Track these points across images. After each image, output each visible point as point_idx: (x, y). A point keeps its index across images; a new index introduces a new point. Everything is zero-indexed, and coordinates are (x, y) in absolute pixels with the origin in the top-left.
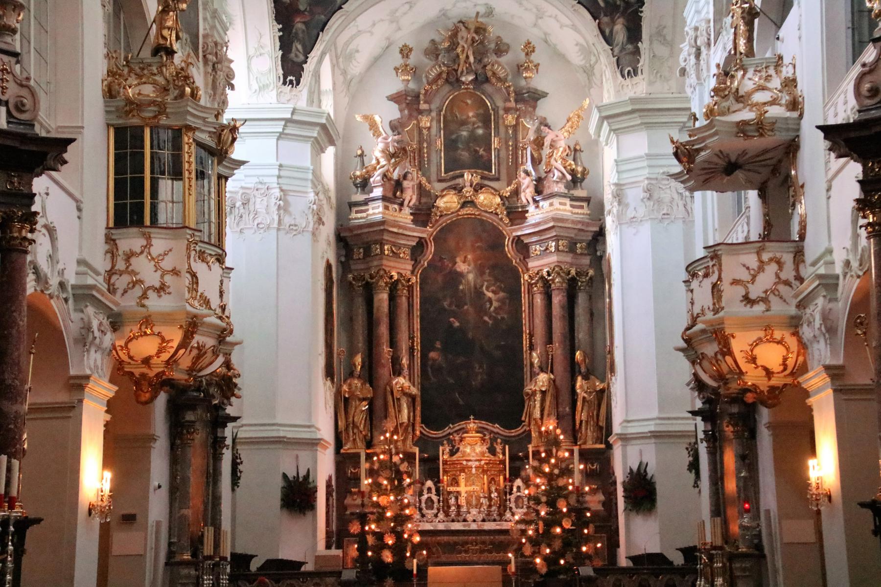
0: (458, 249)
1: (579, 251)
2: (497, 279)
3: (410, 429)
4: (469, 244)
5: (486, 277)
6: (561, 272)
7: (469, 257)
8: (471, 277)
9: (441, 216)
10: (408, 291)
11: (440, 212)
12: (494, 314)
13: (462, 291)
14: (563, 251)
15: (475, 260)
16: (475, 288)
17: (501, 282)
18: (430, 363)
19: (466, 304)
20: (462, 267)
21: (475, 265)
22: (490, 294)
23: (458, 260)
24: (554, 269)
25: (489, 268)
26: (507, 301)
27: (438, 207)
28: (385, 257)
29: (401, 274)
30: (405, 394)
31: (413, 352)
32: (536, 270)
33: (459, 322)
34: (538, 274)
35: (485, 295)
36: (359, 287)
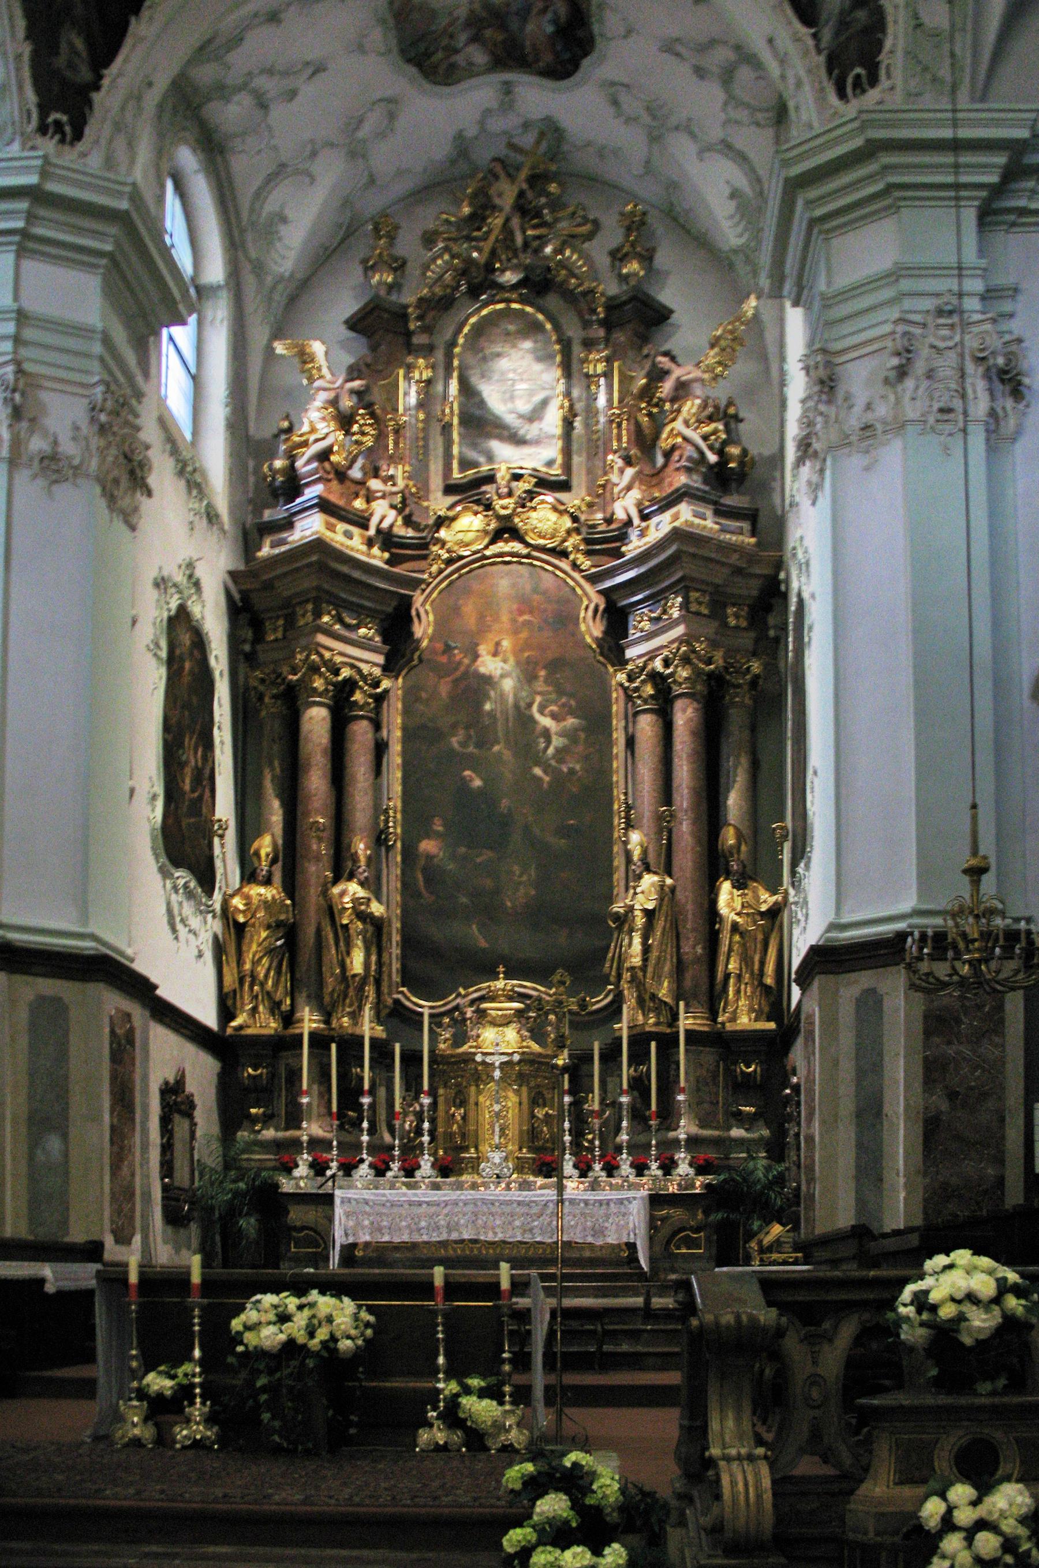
0: (483, 629)
1: (732, 622)
2: (560, 692)
3: (370, 990)
4: (505, 618)
5: (540, 685)
6: (692, 656)
7: (506, 644)
8: (508, 685)
13: (491, 714)
14: (698, 614)
15: (517, 652)
16: (516, 706)
17: (571, 695)
20: (489, 665)
21: (518, 663)
22: (546, 722)
23: (482, 649)
24: (678, 649)
25: (545, 667)
26: (582, 735)
29: (359, 671)
30: (363, 916)
32: (640, 662)
34: (643, 668)
35: (534, 722)
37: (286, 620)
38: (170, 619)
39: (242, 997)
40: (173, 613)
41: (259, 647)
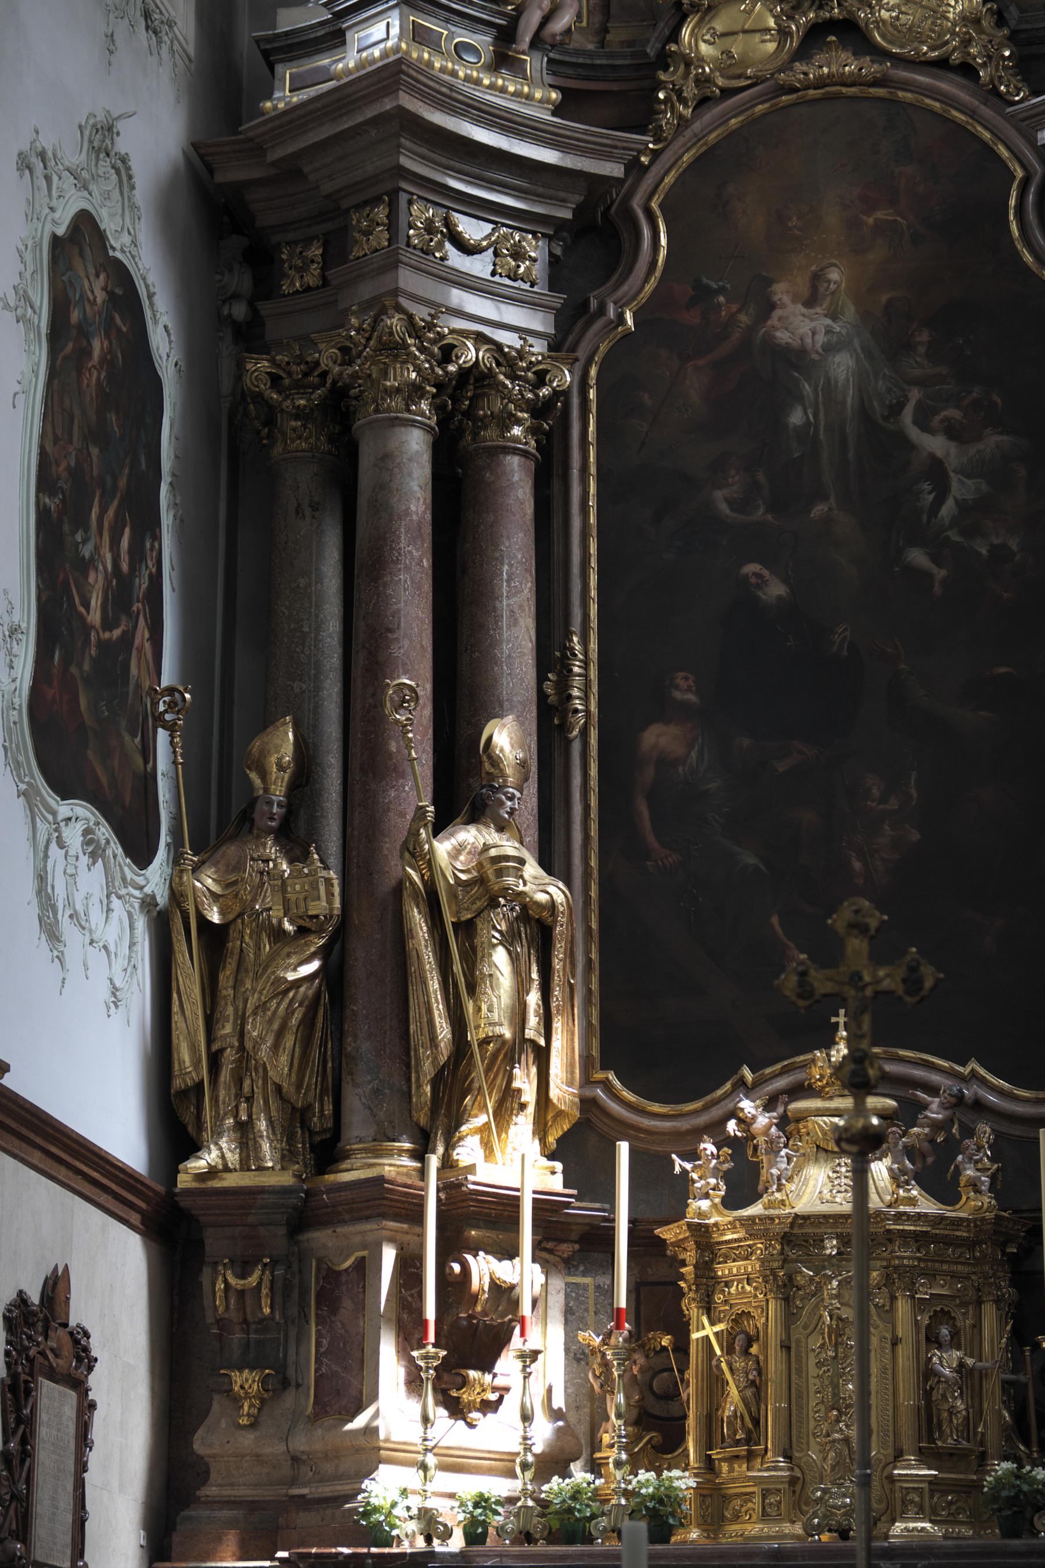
7: (834, 275)
9: (703, 102)
10: (532, 431)
11: (703, 81)
12: (954, 536)
16: (864, 412)
18: (649, 774)
19: (825, 498)
22: (935, 444)
23: (781, 291)
27: (688, 64)
28: (406, 256)
29: (498, 347)
31: (564, 727)
33: (786, 581)
35: (910, 446)
36: (299, 414)
37: (326, 245)
38: (56, 241)
39: (215, 1099)
40: (61, 231)
41: (266, 308)
